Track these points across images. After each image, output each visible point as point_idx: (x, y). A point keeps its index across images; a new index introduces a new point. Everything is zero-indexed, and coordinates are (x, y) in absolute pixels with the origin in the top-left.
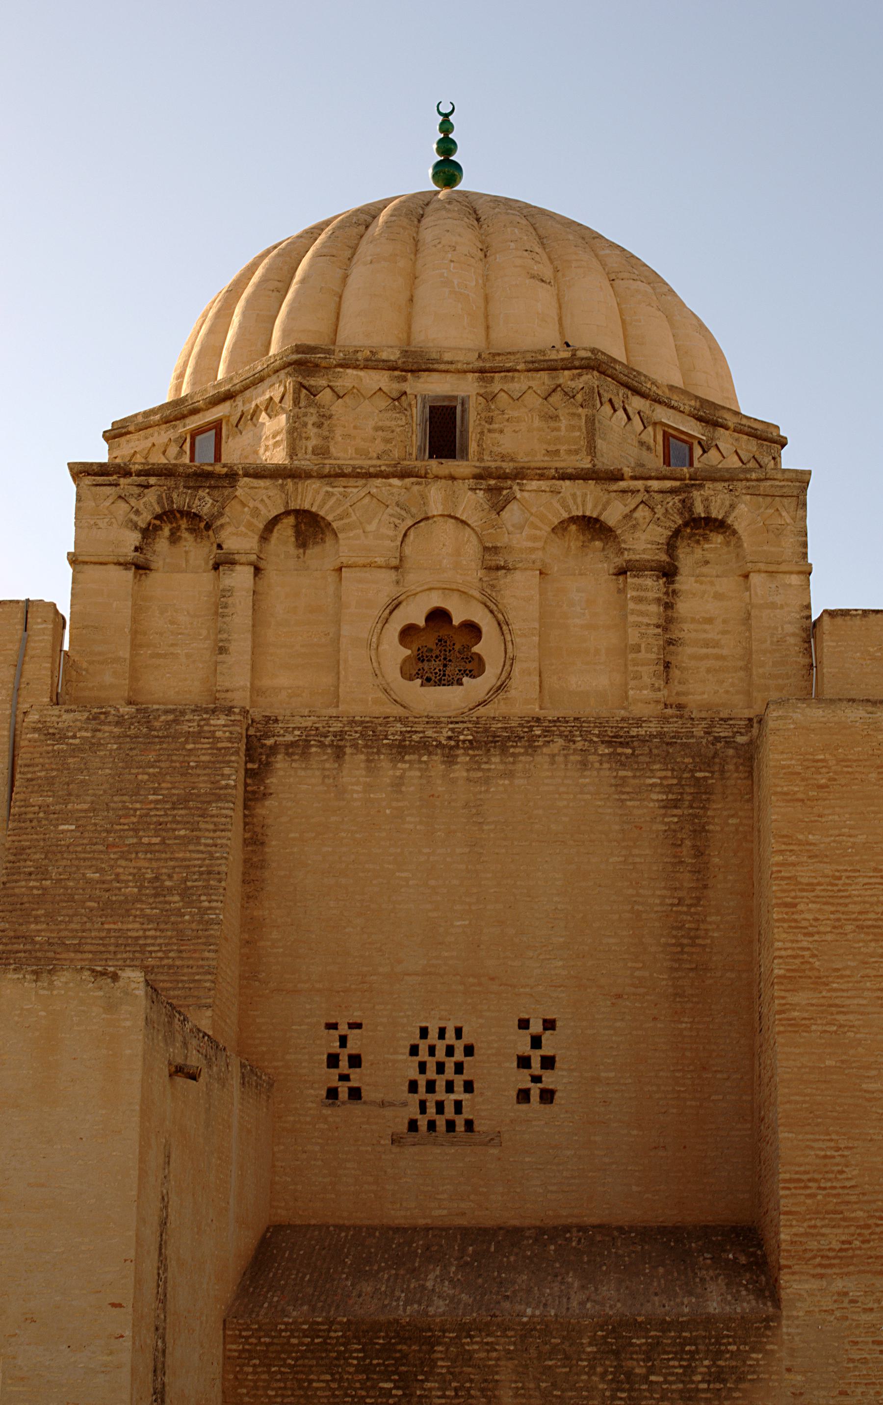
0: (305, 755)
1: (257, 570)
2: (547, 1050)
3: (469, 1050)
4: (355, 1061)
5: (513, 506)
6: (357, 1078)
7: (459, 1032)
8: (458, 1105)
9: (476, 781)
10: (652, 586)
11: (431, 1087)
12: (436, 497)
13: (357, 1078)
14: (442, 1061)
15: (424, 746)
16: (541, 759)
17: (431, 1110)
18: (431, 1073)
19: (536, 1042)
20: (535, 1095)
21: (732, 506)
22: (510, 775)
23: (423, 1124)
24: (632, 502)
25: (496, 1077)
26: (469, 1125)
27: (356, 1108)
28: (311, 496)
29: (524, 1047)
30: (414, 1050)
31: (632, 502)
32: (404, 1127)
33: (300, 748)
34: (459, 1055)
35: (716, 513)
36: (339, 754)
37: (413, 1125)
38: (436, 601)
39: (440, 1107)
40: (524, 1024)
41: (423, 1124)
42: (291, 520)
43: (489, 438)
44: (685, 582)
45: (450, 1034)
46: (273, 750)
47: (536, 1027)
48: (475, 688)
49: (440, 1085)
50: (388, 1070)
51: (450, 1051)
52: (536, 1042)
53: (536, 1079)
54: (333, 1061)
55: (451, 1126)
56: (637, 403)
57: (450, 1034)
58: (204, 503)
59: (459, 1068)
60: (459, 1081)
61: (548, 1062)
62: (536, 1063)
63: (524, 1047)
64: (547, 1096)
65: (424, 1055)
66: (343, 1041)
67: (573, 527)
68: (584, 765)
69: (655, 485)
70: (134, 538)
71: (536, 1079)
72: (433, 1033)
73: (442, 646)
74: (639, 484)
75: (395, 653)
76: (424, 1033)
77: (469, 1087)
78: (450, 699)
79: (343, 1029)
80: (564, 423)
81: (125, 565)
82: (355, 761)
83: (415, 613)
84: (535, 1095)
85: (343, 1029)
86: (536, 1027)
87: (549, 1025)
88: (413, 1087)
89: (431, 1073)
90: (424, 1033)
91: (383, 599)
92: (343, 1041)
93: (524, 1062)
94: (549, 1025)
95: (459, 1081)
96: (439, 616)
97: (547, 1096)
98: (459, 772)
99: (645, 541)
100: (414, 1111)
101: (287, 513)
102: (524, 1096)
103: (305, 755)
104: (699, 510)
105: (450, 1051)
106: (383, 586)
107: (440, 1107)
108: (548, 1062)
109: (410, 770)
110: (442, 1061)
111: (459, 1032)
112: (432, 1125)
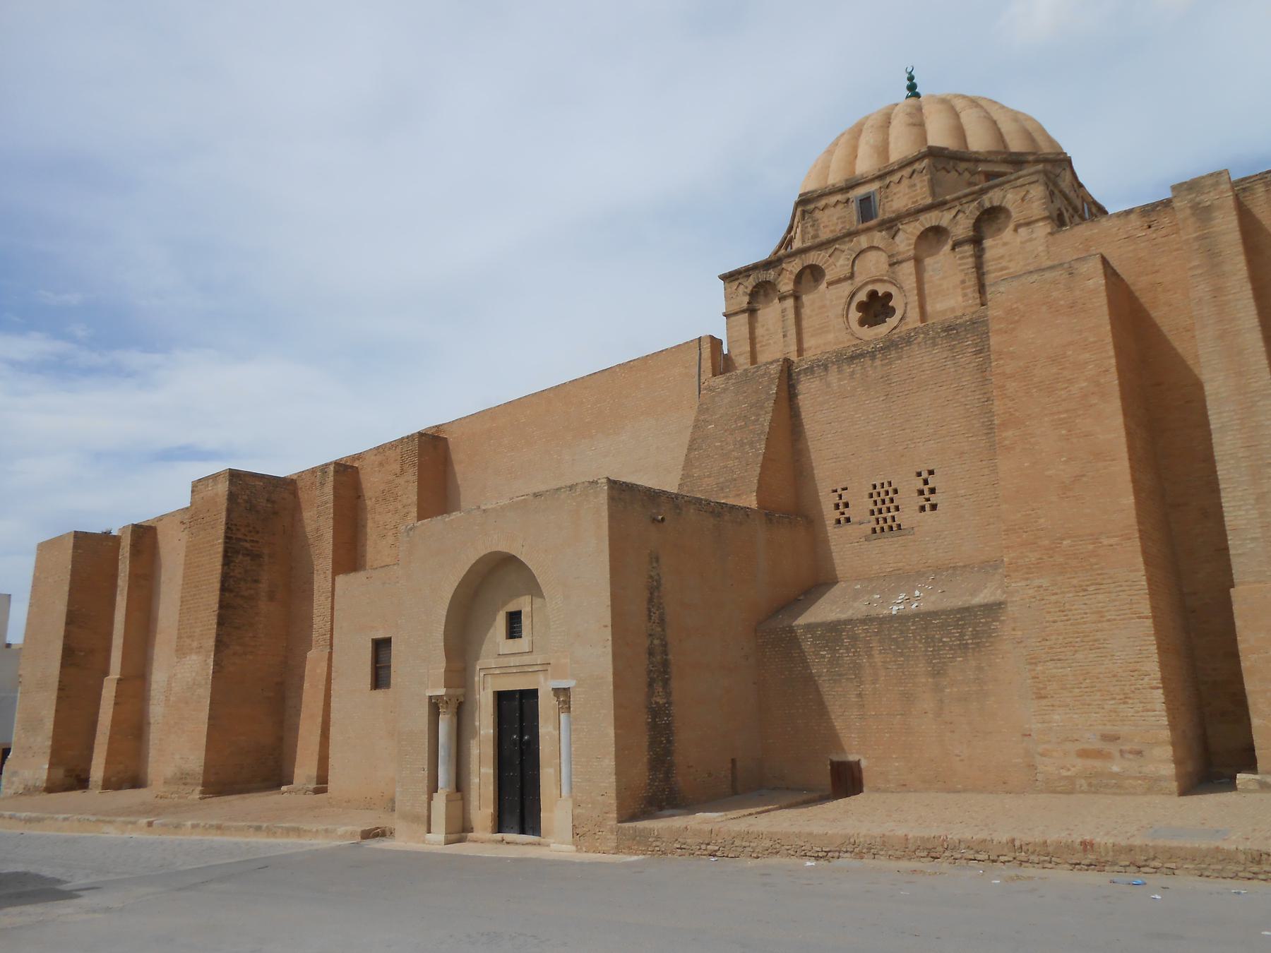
0: (812, 372)
1: (797, 298)
2: (931, 485)
3: (896, 491)
4: (846, 505)
5: (901, 233)
6: (848, 513)
7: (890, 484)
8: (893, 518)
9: (886, 365)
10: (968, 249)
11: (880, 511)
12: (863, 241)
13: (848, 513)
14: (884, 498)
15: (862, 355)
16: (915, 347)
17: (881, 522)
18: (879, 505)
19: (926, 482)
20: (927, 508)
21: (1004, 197)
22: (900, 358)
23: (878, 529)
24: (954, 212)
25: (909, 500)
26: (899, 526)
27: (848, 527)
28: (813, 258)
29: (920, 485)
30: (871, 496)
31: (954, 212)
32: (870, 532)
33: (810, 370)
34: (891, 495)
35: (996, 203)
36: (826, 368)
37: (874, 531)
38: (870, 287)
39: (885, 520)
40: (919, 474)
41: (878, 529)
42: (808, 271)
43: (887, 205)
44: (988, 243)
45: (886, 485)
46: (799, 373)
47: (925, 475)
48: (892, 321)
49: (884, 510)
50: (861, 506)
51: (887, 493)
52: (926, 482)
53: (928, 500)
54: (837, 506)
55: (891, 528)
56: (962, 166)
57: (886, 485)
58: (771, 275)
59: (892, 500)
60: (892, 506)
61: (933, 491)
62: (926, 492)
63: (920, 485)
64: (934, 507)
65: (875, 497)
66: (840, 496)
67: (930, 234)
68: (934, 344)
69: (964, 201)
70: (746, 299)
71: (928, 500)
72: (878, 486)
73: (876, 308)
74: (957, 203)
75: (855, 315)
76: (875, 487)
77: (897, 509)
78: (882, 330)
79: (840, 491)
80: (918, 186)
81: (743, 311)
82: (833, 369)
83: (862, 296)
84: (927, 508)
85: (840, 491)
86: (925, 475)
87: (931, 472)
88: (872, 513)
89: (879, 505)
90: (875, 487)
91: (847, 293)
92: (840, 496)
93: (921, 492)
94: (931, 472)
95: (892, 506)
96: (873, 294)
97: (934, 507)
98: (878, 362)
99: (962, 228)
100: (873, 524)
101: (804, 268)
102: (923, 509)
103: (812, 372)
104: (987, 205)
105: (887, 493)
106: (846, 288)
107: (885, 520)
108: (933, 491)
109: (856, 367)
110: (884, 498)
111: (890, 484)
112: (882, 529)
